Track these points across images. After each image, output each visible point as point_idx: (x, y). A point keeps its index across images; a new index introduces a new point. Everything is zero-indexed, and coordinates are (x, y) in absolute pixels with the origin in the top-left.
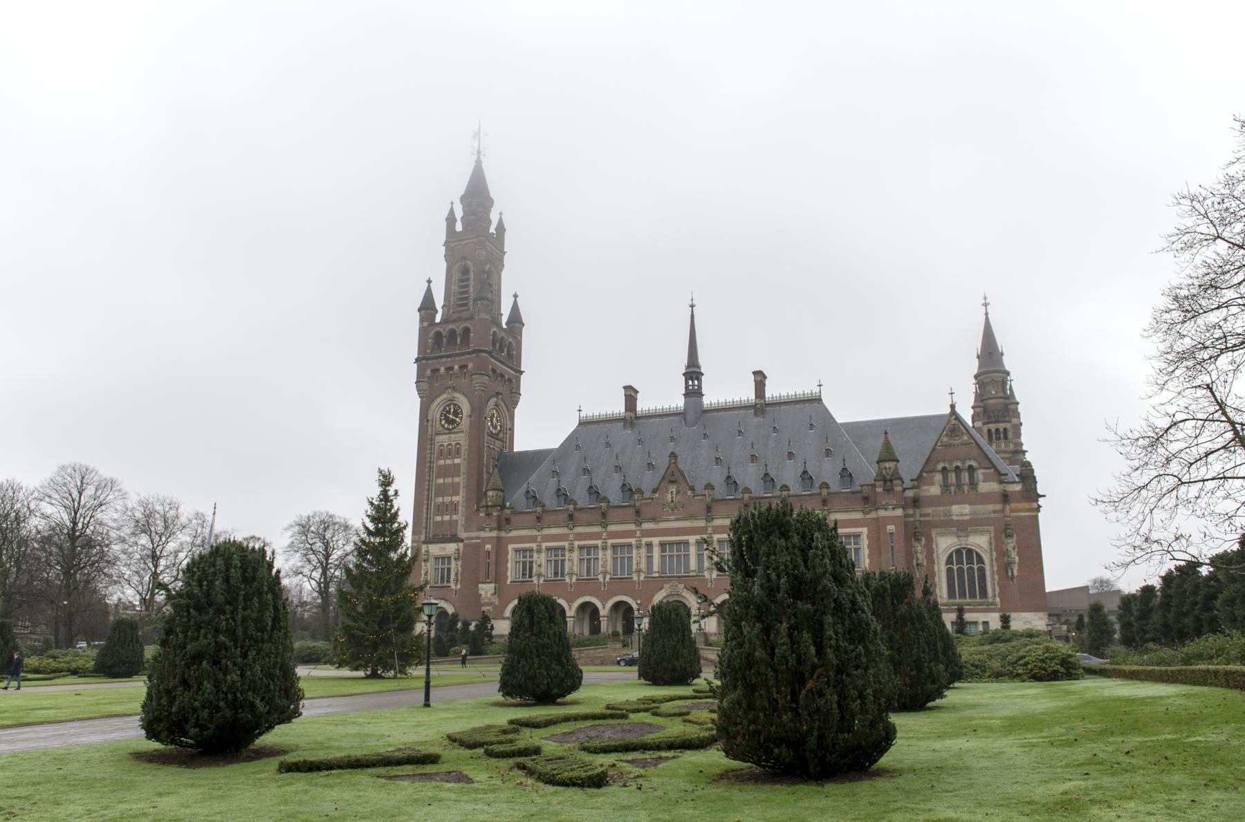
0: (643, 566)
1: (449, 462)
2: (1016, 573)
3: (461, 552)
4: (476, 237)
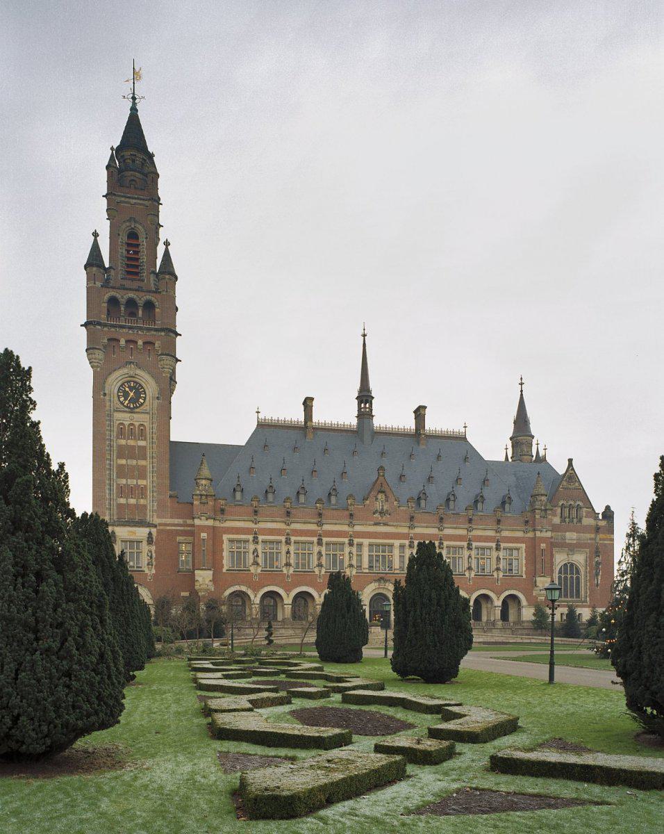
0: (354, 562)
1: (131, 443)
3: (154, 537)
4: (149, 200)
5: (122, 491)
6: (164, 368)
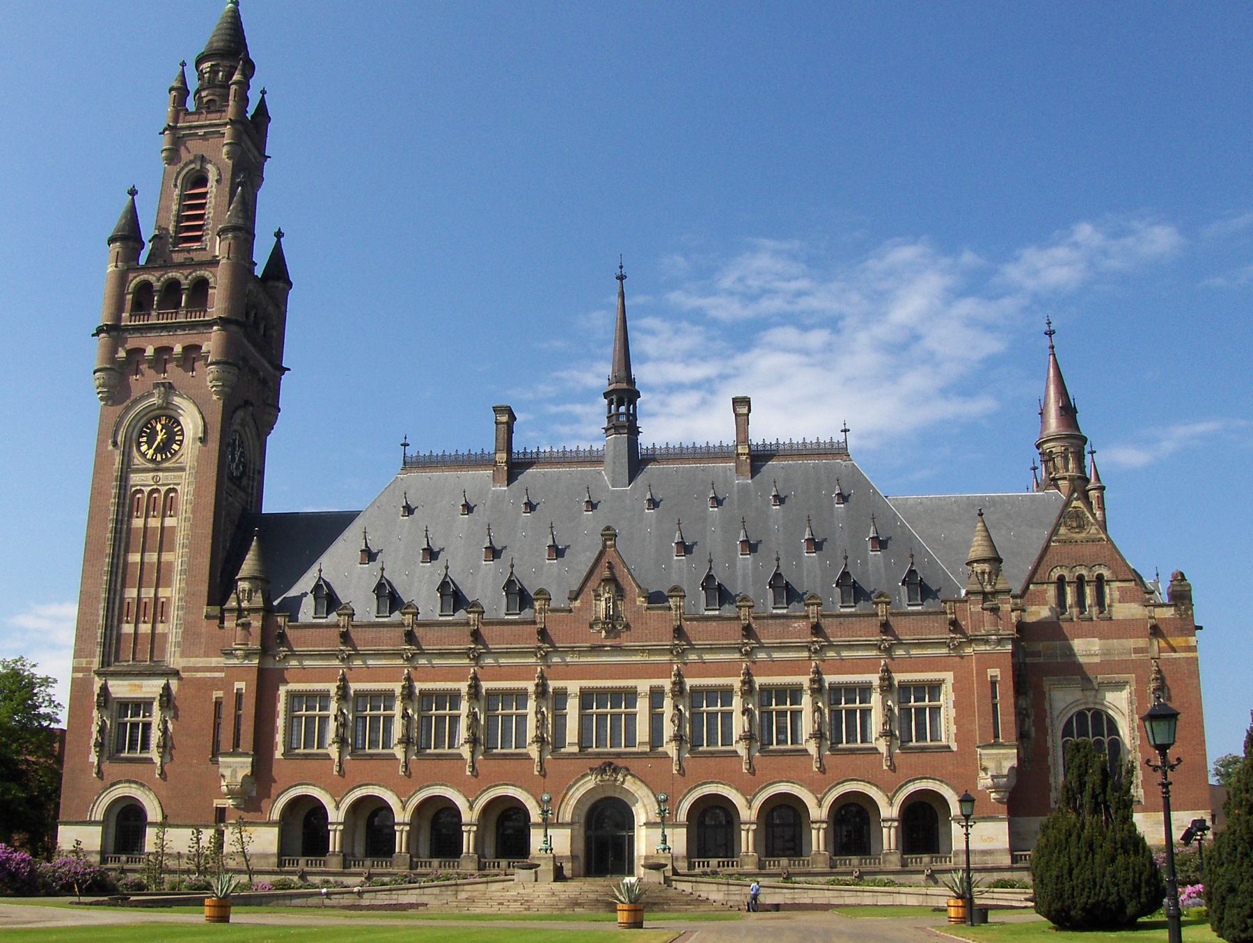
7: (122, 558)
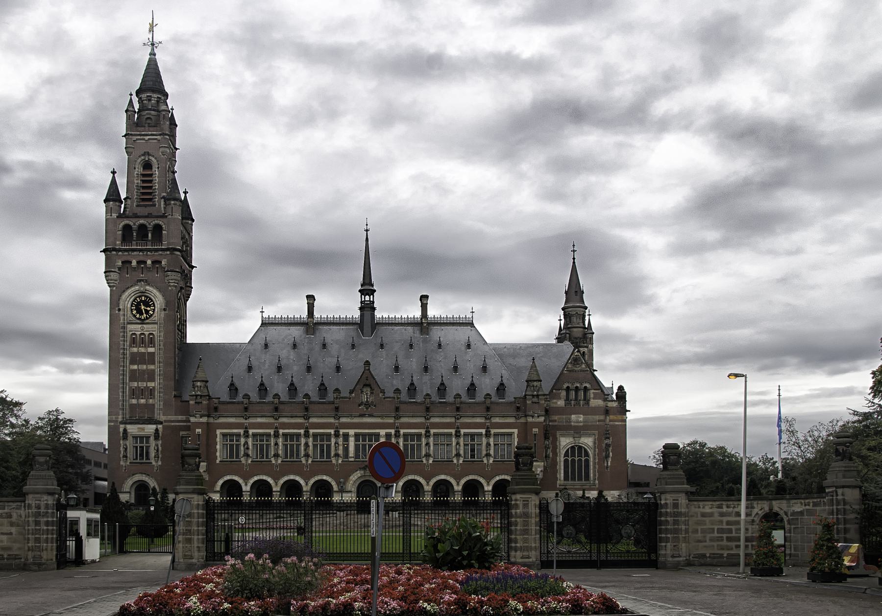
0: (340, 452)
2: (609, 464)
3: (160, 435)
4: (160, 135)
5: (134, 393)
6: (169, 283)
7: (128, 367)
